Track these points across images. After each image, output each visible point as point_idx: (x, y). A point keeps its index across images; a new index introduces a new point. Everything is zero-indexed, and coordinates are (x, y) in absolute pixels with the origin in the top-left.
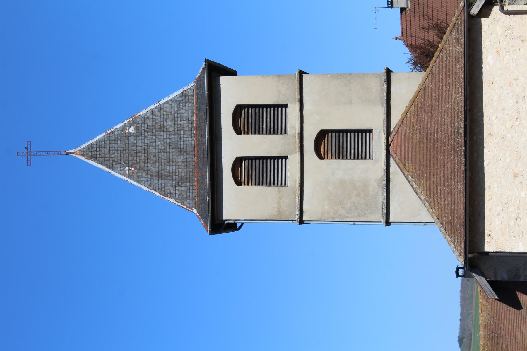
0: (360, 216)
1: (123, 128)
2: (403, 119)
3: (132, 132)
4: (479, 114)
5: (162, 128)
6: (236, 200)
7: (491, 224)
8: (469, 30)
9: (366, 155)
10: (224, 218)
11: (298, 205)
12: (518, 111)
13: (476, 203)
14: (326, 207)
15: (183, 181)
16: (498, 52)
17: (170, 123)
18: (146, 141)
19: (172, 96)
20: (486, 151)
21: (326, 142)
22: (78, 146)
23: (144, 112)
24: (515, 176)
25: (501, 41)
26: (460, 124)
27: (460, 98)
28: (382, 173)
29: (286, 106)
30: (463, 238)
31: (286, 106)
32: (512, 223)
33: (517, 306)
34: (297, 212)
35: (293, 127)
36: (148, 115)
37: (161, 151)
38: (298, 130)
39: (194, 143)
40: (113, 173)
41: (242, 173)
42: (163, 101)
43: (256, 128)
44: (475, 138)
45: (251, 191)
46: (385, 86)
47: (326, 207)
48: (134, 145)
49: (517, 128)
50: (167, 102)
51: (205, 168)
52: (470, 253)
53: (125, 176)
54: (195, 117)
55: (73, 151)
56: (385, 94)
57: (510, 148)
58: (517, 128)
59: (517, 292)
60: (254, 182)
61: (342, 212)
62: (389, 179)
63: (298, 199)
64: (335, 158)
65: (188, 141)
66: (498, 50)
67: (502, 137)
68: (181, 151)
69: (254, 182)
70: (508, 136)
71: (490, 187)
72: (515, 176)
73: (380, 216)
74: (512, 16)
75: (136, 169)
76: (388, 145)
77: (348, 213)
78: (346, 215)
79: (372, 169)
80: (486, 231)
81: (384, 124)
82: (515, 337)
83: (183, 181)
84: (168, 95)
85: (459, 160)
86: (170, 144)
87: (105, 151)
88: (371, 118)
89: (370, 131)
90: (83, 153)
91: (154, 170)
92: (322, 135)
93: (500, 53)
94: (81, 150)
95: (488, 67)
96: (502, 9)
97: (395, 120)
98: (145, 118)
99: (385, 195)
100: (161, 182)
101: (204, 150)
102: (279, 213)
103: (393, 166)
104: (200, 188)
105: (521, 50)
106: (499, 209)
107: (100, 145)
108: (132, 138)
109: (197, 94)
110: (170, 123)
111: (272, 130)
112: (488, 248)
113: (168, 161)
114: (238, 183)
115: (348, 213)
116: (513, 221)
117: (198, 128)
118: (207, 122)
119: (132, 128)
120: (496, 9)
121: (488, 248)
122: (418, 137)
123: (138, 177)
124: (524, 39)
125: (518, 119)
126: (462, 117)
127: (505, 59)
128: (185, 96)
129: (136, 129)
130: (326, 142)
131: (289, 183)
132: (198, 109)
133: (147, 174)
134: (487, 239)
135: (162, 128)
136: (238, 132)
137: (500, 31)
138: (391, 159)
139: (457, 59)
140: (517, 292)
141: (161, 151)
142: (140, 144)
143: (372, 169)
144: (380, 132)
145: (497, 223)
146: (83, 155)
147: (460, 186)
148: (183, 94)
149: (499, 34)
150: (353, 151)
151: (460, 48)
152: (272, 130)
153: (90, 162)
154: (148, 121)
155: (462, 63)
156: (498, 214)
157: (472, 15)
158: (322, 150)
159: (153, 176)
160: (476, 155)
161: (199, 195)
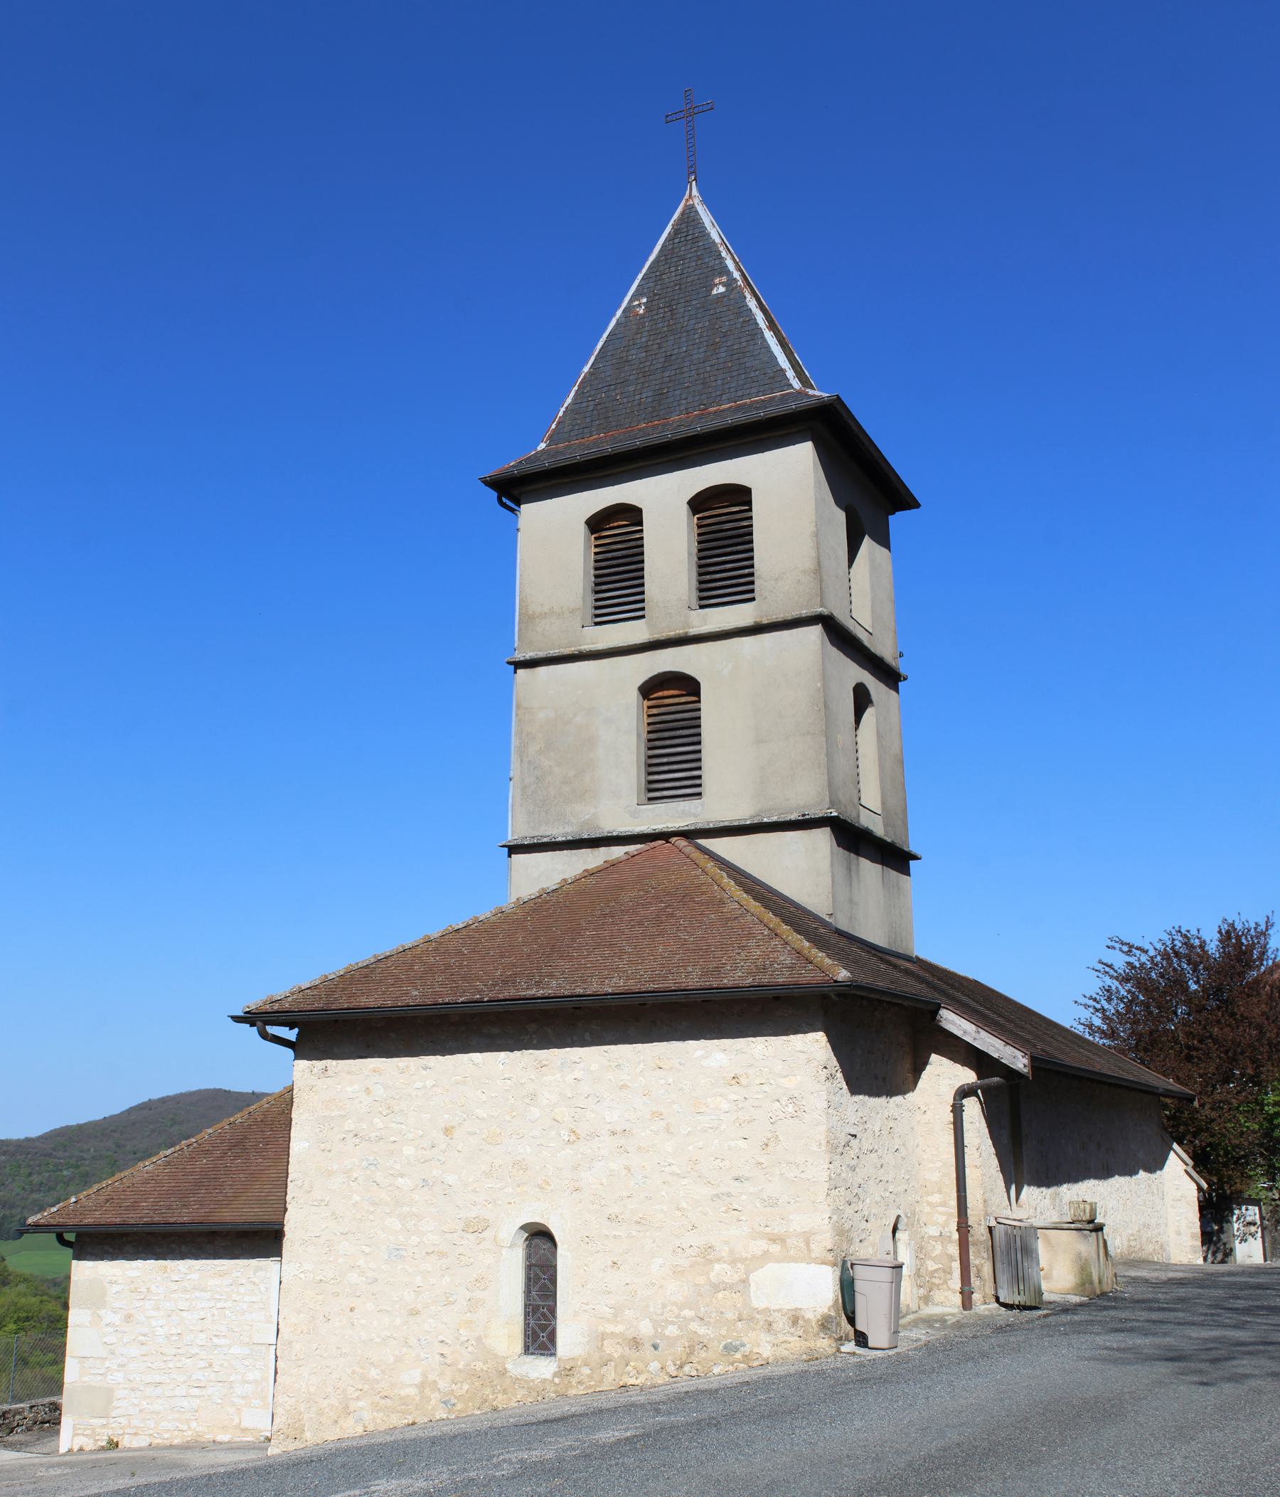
1: (724, 271)
3: (714, 292)
4: (587, 1036)
6: (555, 530)
7: (349, 1073)
8: (777, 998)
9: (655, 790)
11: (541, 654)
12: (594, 1135)
13: (393, 1035)
14: (541, 715)
20: (503, 1055)
21: (683, 699)
22: (705, 201)
24: (448, 1131)
25: (765, 1088)
32: (349, 1125)
34: (530, 655)
38: (693, 631)
40: (640, 276)
44: (532, 1027)
46: (794, 816)
47: (541, 715)
49: (553, 1133)
53: (631, 301)
55: (695, 192)
56: (775, 819)
57: (508, 1118)
58: (553, 1133)
60: (600, 557)
61: (533, 749)
62: (598, 847)
64: (649, 724)
66: (743, 1081)
67: (533, 1096)
69: (600, 557)
70: (535, 1112)
71: (425, 1068)
72: (448, 1131)
73: (518, 831)
74: (950, 1117)
75: (643, 316)
76: (665, 836)
77: (529, 762)
78: (526, 759)
79: (621, 806)
80: (334, 1062)
81: (708, 823)
88: (726, 791)
90: (690, 209)
92: (688, 685)
93: (736, 1088)
94: (693, 206)
95: (698, 1053)
96: (965, 1092)
97: (718, 846)
99: (560, 839)
102: (529, 619)
105: (742, 1143)
111: (708, 577)
115: (529, 762)
116: (352, 1127)
120: (968, 1076)
124: (770, 1149)
125: (573, 1138)
127: (719, 1099)
130: (683, 699)
143: (621, 806)
144: (696, 816)
145: (349, 1089)
149: (784, 1082)
150: (665, 760)
152: (708, 577)
153: (669, 228)
157: (936, 1012)
158: (666, 693)
160: (495, 1031)
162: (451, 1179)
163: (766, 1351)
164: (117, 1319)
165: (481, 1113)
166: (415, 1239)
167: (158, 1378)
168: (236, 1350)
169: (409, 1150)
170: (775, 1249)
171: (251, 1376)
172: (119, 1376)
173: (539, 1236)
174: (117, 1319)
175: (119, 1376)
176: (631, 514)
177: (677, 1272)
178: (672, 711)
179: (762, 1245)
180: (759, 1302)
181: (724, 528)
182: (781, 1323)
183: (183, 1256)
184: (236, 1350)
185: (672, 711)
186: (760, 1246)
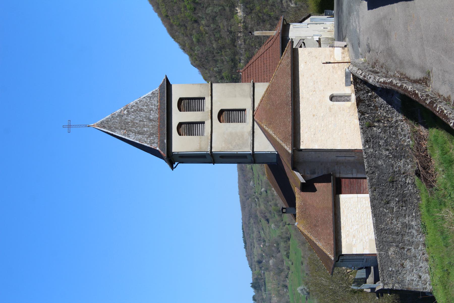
0: (240, 149)
2: (259, 105)
5: (141, 110)
10: (173, 151)
11: (210, 144)
12: (315, 88)
14: (223, 145)
15: (152, 134)
16: (306, 62)
17: (146, 107)
18: (133, 117)
23: (132, 103)
24: (314, 116)
26: (289, 93)
27: (289, 81)
28: (250, 129)
29: (204, 98)
30: (291, 141)
31: (204, 98)
32: (312, 136)
33: (314, 190)
34: (209, 147)
35: (208, 108)
36: (134, 104)
37: (140, 121)
39: (158, 116)
41: (181, 130)
42: (142, 97)
43: (189, 109)
45: (186, 138)
46: (252, 89)
47: (223, 145)
48: (126, 119)
50: (144, 98)
51: (164, 126)
52: (294, 147)
61: (231, 147)
63: (209, 141)
65: (154, 115)
68: (151, 120)
70: (310, 98)
72: (314, 116)
76: (253, 116)
82: (313, 206)
83: (152, 134)
86: (145, 117)
87: (110, 123)
88: (246, 104)
89: (244, 110)
91: (137, 131)
92: (221, 112)
94: (97, 124)
97: (256, 105)
98: (132, 106)
100: (140, 136)
101: (164, 118)
102: (200, 148)
103: (256, 126)
104: (161, 137)
108: (125, 116)
110: (146, 107)
112: (302, 147)
113: (144, 126)
114: (180, 134)
118: (166, 104)
119: (125, 111)
121: (302, 147)
122: (268, 106)
123: (128, 135)
126: (290, 89)
128: (154, 94)
129: (128, 111)
131: (205, 134)
132: (160, 100)
133: (133, 133)
135: (141, 110)
137: (306, 54)
138: (255, 122)
139: (288, 65)
141: (140, 121)
142: (129, 118)
146: (98, 126)
147: (289, 120)
148: (153, 93)
151: (289, 60)
154: (134, 107)
155: (290, 66)
156: (306, 133)
159: (136, 133)
161: (160, 141)
162: (322, 114)
164: (354, 240)
165: (310, 109)
166: (333, 122)
167: (366, 227)
168: (359, 206)
170: (332, 56)
171: (364, 202)
172: (367, 237)
173: (332, 98)
174: (354, 240)
175: (367, 237)
176: (180, 125)
177: (336, 73)
178: (226, 115)
179: (332, 58)
181: (186, 104)
182: (344, 55)
183: (340, 222)
184: (359, 206)
185: (226, 115)
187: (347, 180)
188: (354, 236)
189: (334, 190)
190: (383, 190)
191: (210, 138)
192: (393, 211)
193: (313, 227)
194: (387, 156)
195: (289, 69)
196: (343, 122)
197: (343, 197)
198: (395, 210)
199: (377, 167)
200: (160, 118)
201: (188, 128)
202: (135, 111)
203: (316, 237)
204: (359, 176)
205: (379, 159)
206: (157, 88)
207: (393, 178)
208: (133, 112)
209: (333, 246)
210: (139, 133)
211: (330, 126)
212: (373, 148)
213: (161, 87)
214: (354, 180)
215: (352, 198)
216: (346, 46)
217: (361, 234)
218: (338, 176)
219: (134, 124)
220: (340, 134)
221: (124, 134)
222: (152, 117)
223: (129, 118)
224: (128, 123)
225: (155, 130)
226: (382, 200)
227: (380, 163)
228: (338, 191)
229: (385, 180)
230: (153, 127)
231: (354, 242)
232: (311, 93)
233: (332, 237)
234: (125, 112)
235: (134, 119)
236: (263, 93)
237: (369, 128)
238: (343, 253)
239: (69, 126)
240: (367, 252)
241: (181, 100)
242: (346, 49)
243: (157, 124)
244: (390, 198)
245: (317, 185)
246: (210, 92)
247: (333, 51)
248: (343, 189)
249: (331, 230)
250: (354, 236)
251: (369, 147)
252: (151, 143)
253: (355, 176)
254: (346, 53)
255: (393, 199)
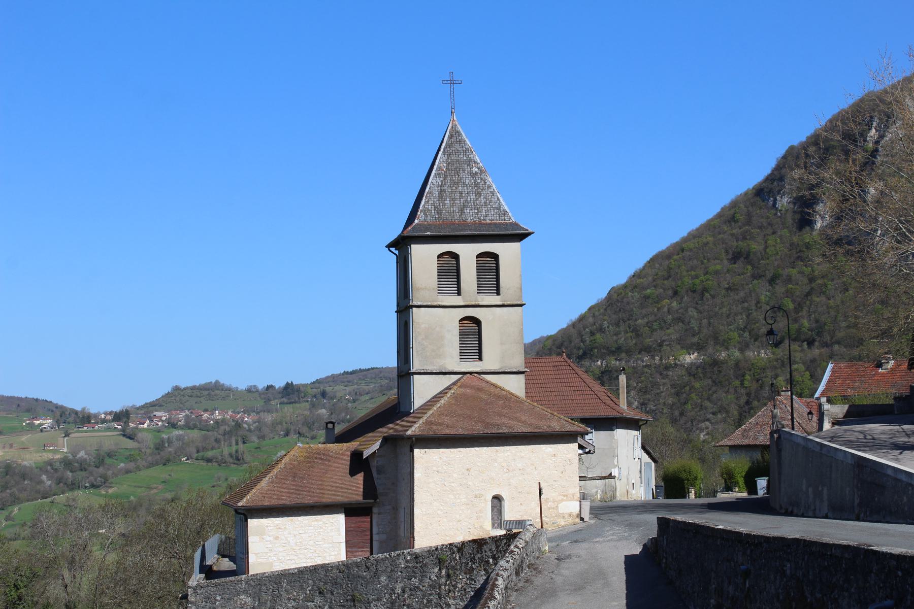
11: (425, 304)
14: (423, 326)
15: (439, 212)
19: (503, 203)
23: (490, 180)
24: (468, 470)
26: (505, 430)
29: (498, 293)
30: (425, 433)
31: (498, 293)
32: (435, 468)
33: (353, 473)
34: (419, 303)
35: (483, 300)
37: (461, 193)
41: (447, 259)
43: (481, 270)
45: (433, 266)
46: (515, 370)
48: (464, 171)
51: (453, 230)
54: (488, 221)
59: (362, 473)
63: (429, 304)
65: (470, 216)
68: (462, 210)
72: (468, 470)
76: (471, 373)
82: (327, 472)
83: (439, 212)
84: (504, 200)
85: (479, 430)
86: (467, 200)
87: (457, 146)
88: (490, 361)
89: (480, 359)
92: (477, 322)
97: (488, 377)
98: (485, 181)
100: (436, 194)
101: (465, 230)
102: (418, 289)
103: (455, 378)
104: (435, 226)
106: (445, 458)
107: (461, 141)
109: (507, 224)
112: (417, 452)
113: (453, 199)
114: (439, 256)
117: (481, 224)
121: (417, 452)
122: (484, 396)
123: (439, 174)
126: (511, 431)
129: (476, 173)
131: (441, 297)
132: (495, 224)
134: (424, 450)
135: (478, 194)
136: (478, 256)
137: (569, 456)
139: (549, 426)
140: (362, 473)
147: (461, 430)
148: (505, 212)
151: (558, 429)
155: (548, 430)
162: (470, 483)
163: (563, 523)
164: (271, 538)
168: (326, 545)
169: (455, 475)
172: (275, 558)
173: (497, 499)
174: (271, 538)
175: (275, 558)
176: (455, 256)
178: (472, 330)
180: (561, 511)
181: (489, 266)
184: (326, 545)
185: (472, 330)
186: (560, 498)
187: (369, 525)
188: (277, 538)
189: (351, 504)
190: (341, 585)
191: (435, 304)
192: (308, 601)
193: (293, 472)
194: (393, 590)
195: (543, 428)
196: (458, 516)
197: (339, 520)
198: (309, 604)
199: (376, 574)
200: (465, 225)
201: (450, 269)
202: (477, 184)
203: (276, 476)
204: (375, 544)
205: (389, 577)
206: (513, 219)
207: (360, 601)
208: (475, 181)
209: (260, 504)
210: (441, 192)
211: (451, 496)
212: (407, 567)
213: (516, 225)
214: (369, 537)
215: (340, 535)
216: (582, 519)
217: (281, 549)
218: (375, 510)
219: (456, 183)
220: (439, 512)
221: (439, 168)
222: (467, 211)
223: (465, 176)
224: (458, 173)
225: (446, 217)
226: (325, 583)
227: (383, 579)
228: (351, 511)
229: (356, 588)
230: (452, 214)
231: (268, 538)
232: (504, 464)
233: (274, 502)
234: (475, 170)
235: (464, 183)
236: (507, 388)
237: (437, 561)
238: (249, 520)
239: (452, 82)
240: (252, 559)
241: (495, 257)
242: (578, 520)
243: (456, 219)
244: (329, 595)
245: (360, 477)
246: (509, 303)
247: (573, 499)
248: (354, 519)
249: (286, 500)
250: (277, 538)
251: (407, 561)
252: (425, 211)
253: (375, 537)
254: (570, 521)
255: (326, 601)
